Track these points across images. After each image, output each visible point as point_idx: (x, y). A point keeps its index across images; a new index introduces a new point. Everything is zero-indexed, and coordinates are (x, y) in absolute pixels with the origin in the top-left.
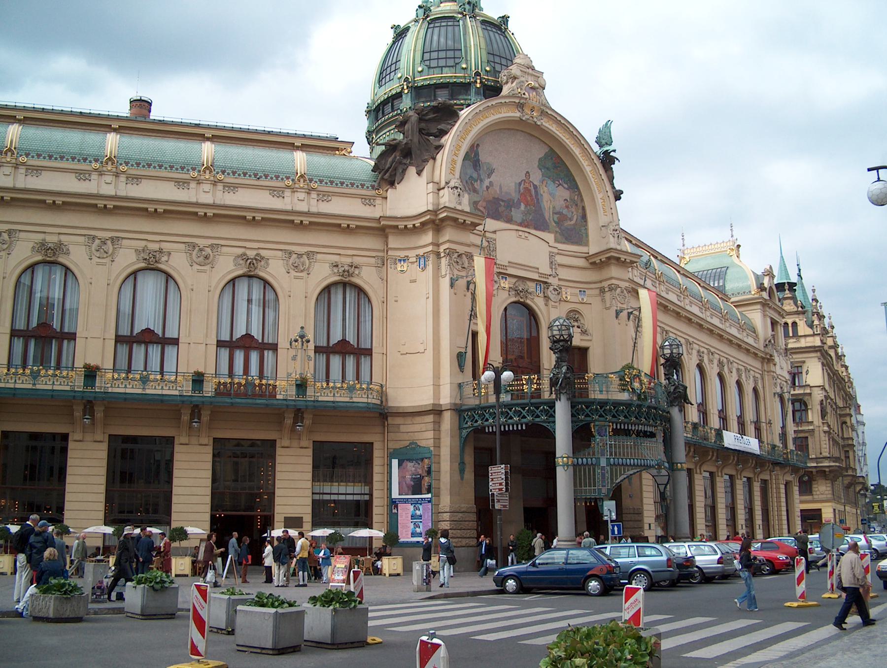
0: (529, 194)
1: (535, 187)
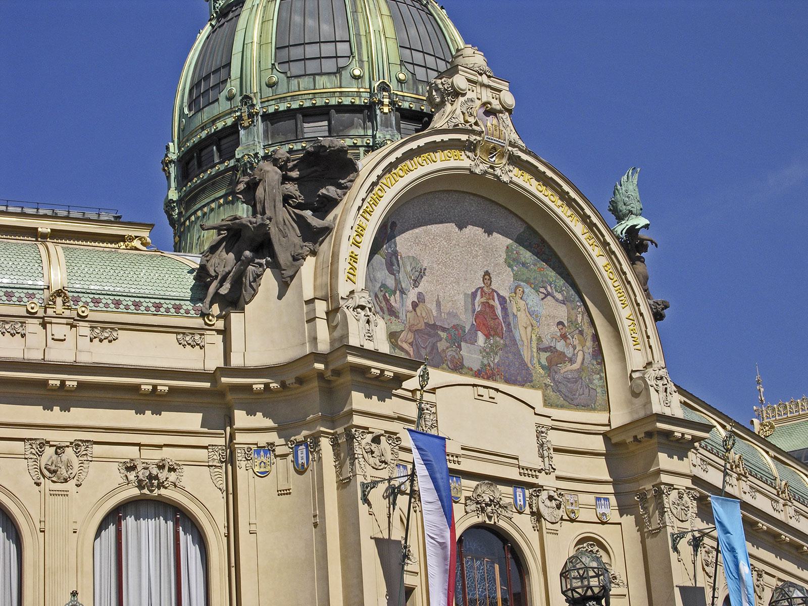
0: (491, 318)
1: (503, 300)
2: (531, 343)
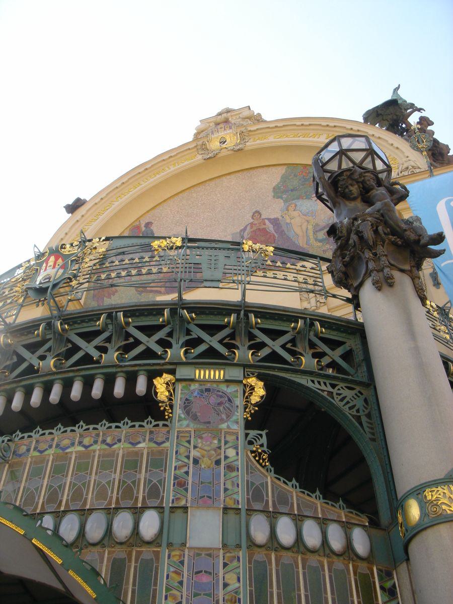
1: (275, 222)
2: (306, 232)
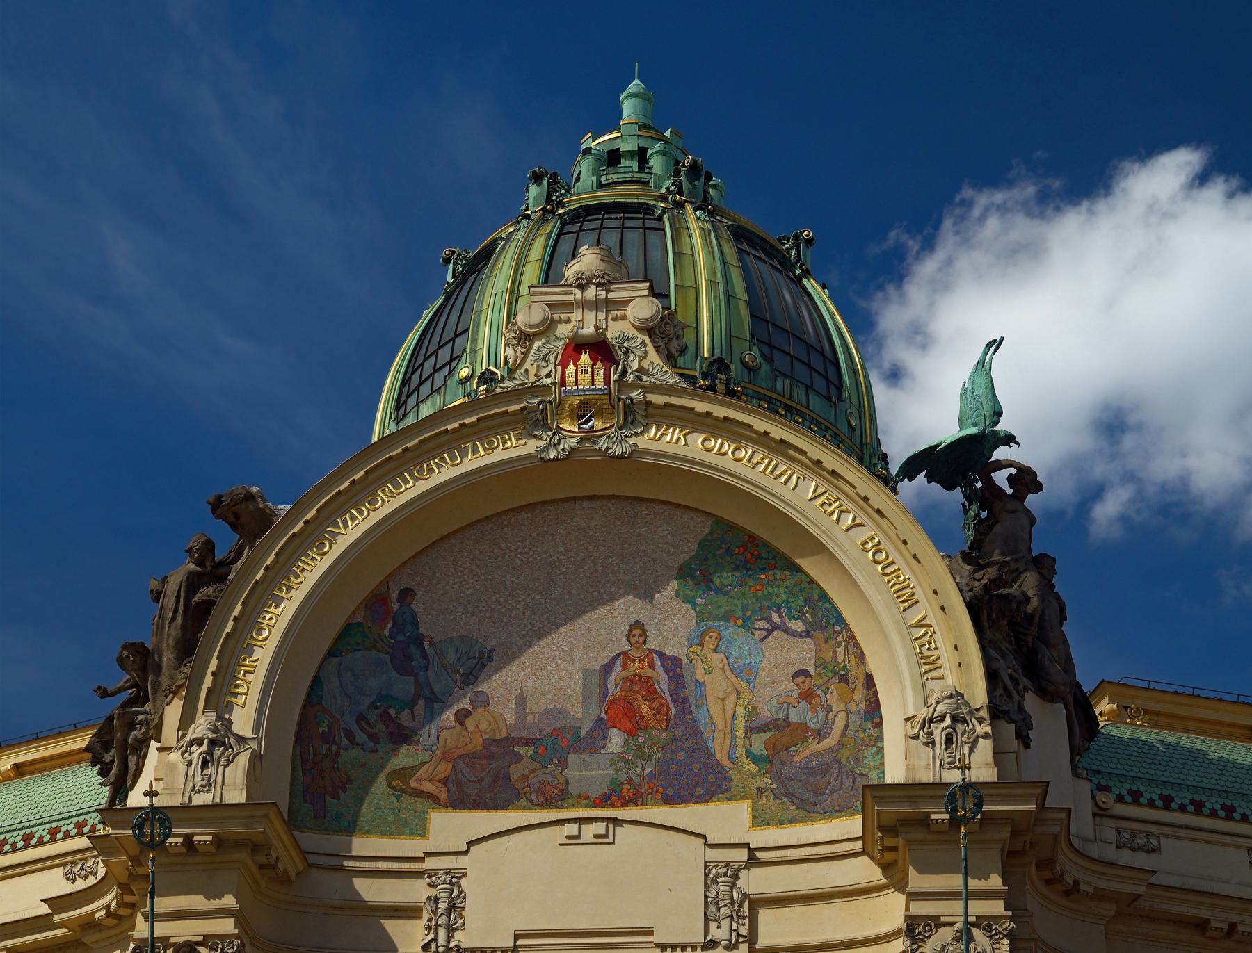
1: (673, 665)
2: (732, 723)
